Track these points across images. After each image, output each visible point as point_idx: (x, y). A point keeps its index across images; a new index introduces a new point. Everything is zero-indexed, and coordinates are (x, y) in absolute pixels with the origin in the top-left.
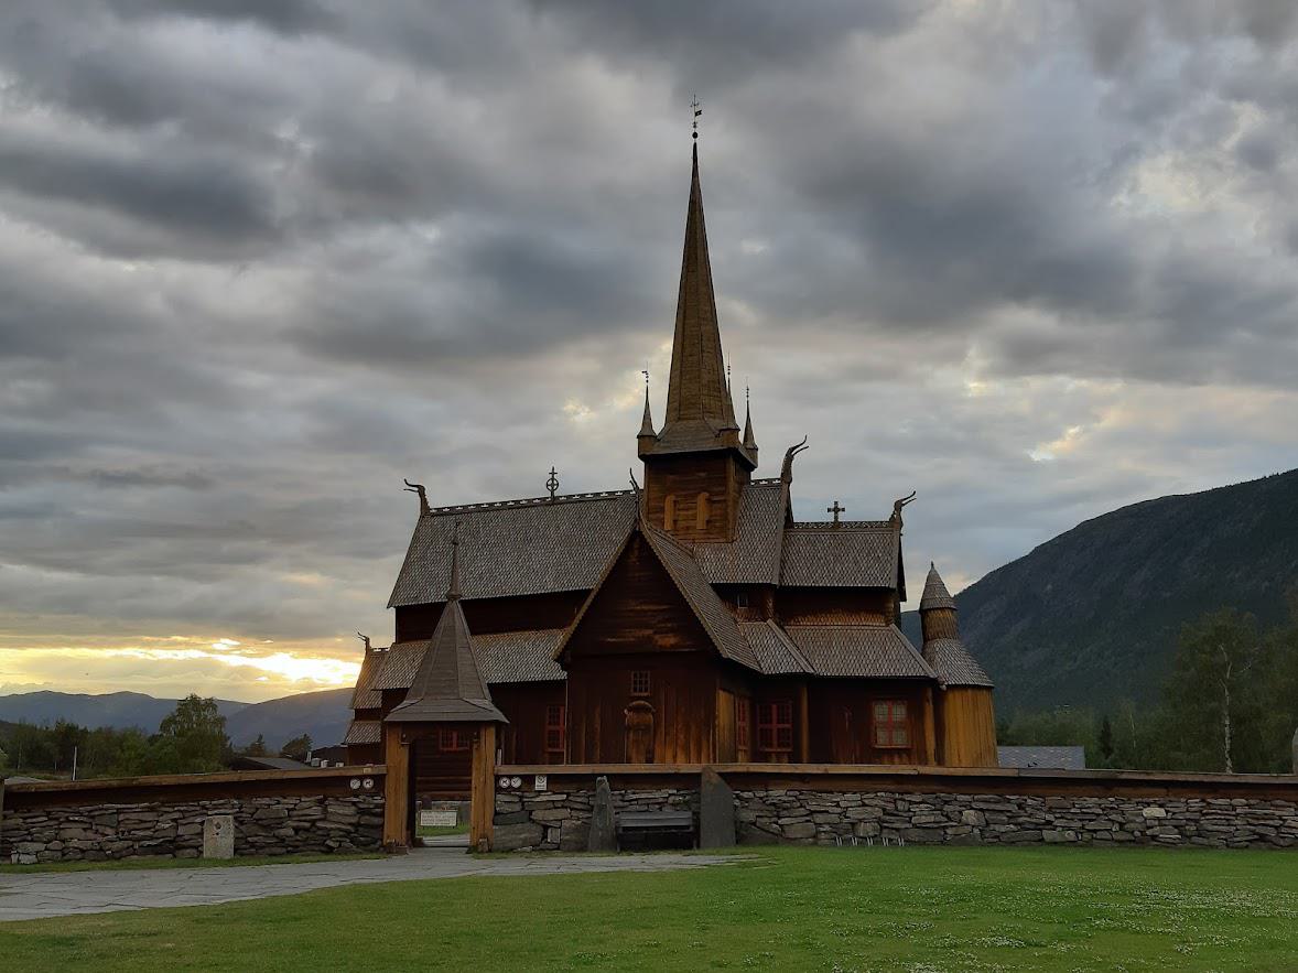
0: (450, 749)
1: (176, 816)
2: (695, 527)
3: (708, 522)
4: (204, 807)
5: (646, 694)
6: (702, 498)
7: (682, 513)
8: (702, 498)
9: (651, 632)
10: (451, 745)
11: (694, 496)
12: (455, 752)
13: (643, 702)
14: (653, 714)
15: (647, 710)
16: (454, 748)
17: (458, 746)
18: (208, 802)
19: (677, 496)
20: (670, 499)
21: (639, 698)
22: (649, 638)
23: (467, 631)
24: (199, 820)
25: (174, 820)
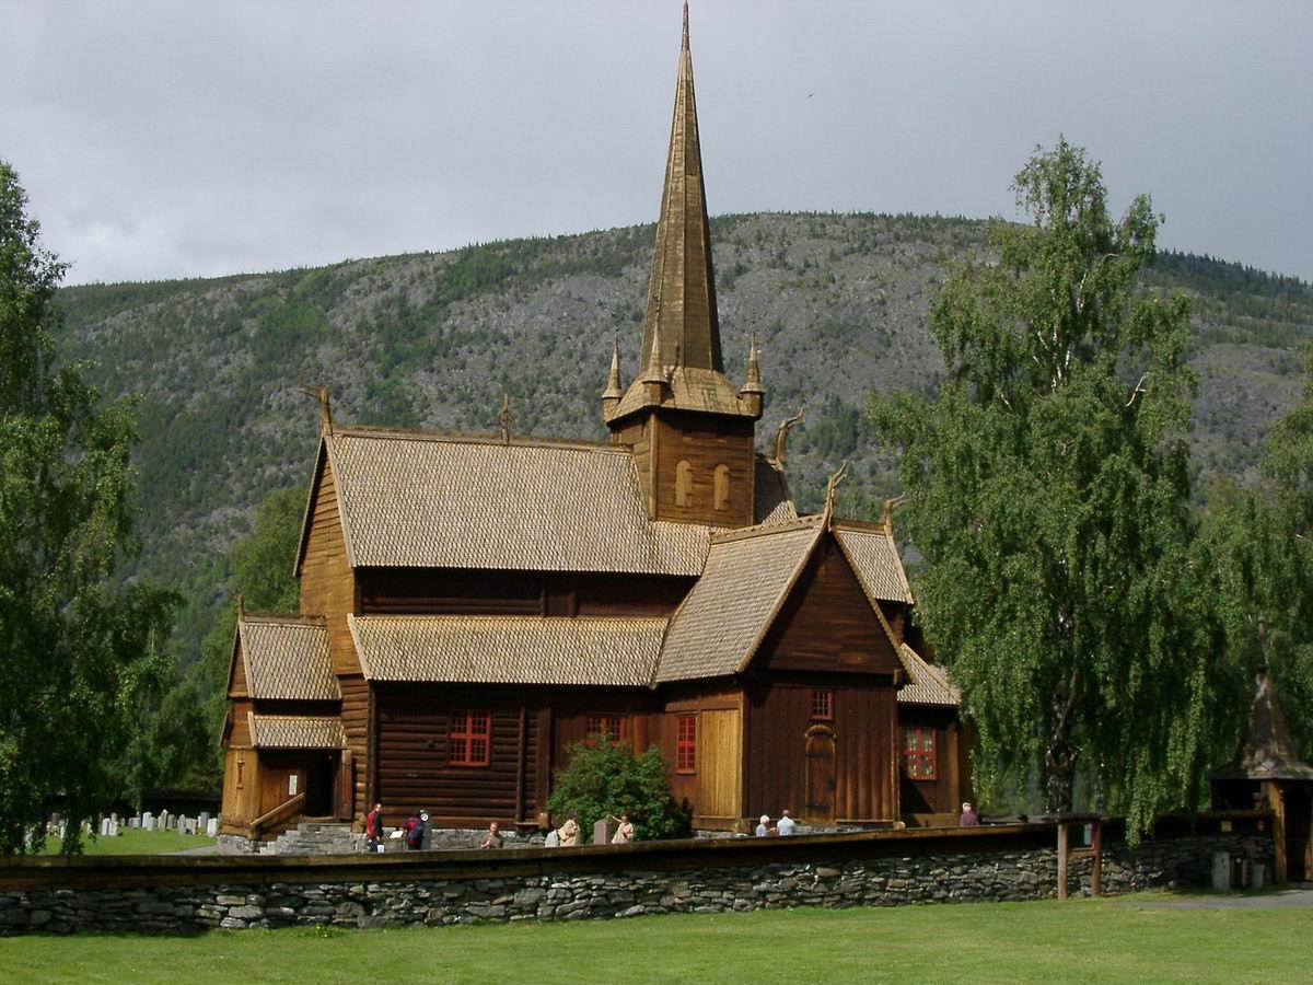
0: (461, 763)
1: (1162, 851)
2: (713, 505)
3: (727, 502)
4: (1177, 844)
5: (824, 717)
6: (721, 470)
7: (698, 486)
8: (721, 470)
9: (837, 647)
10: (464, 759)
11: (713, 468)
12: (468, 768)
13: (824, 727)
14: (835, 741)
15: (830, 736)
16: (467, 762)
17: (472, 759)
18: (1178, 840)
19: (691, 465)
20: (683, 466)
21: (819, 722)
22: (836, 653)
23: (350, 597)
24: (1175, 855)
25: (1162, 855)
